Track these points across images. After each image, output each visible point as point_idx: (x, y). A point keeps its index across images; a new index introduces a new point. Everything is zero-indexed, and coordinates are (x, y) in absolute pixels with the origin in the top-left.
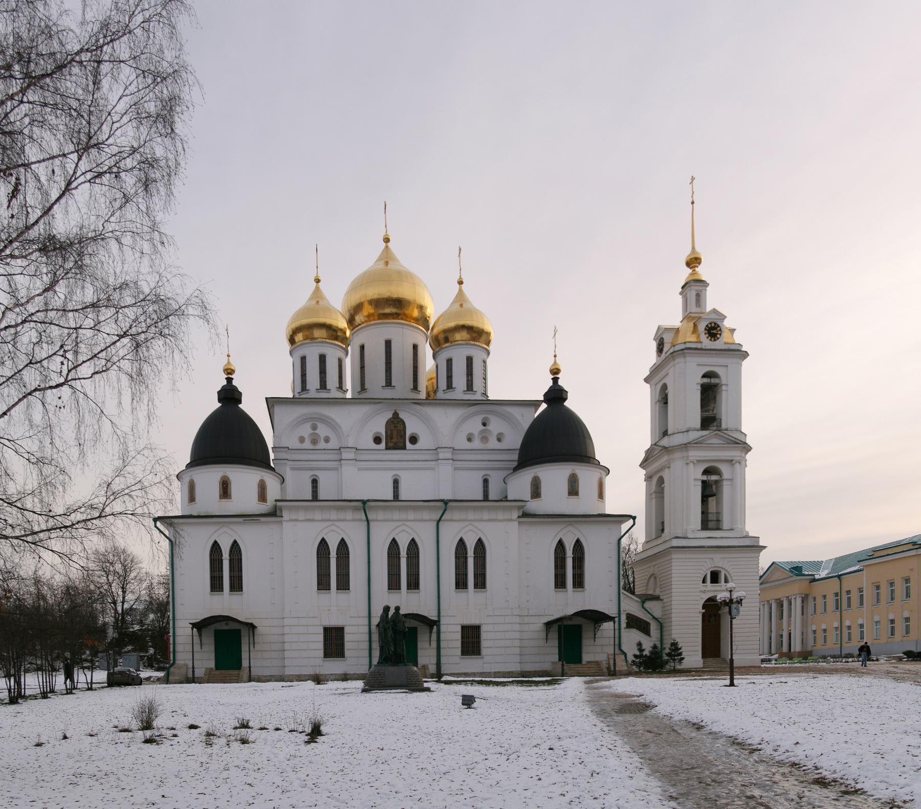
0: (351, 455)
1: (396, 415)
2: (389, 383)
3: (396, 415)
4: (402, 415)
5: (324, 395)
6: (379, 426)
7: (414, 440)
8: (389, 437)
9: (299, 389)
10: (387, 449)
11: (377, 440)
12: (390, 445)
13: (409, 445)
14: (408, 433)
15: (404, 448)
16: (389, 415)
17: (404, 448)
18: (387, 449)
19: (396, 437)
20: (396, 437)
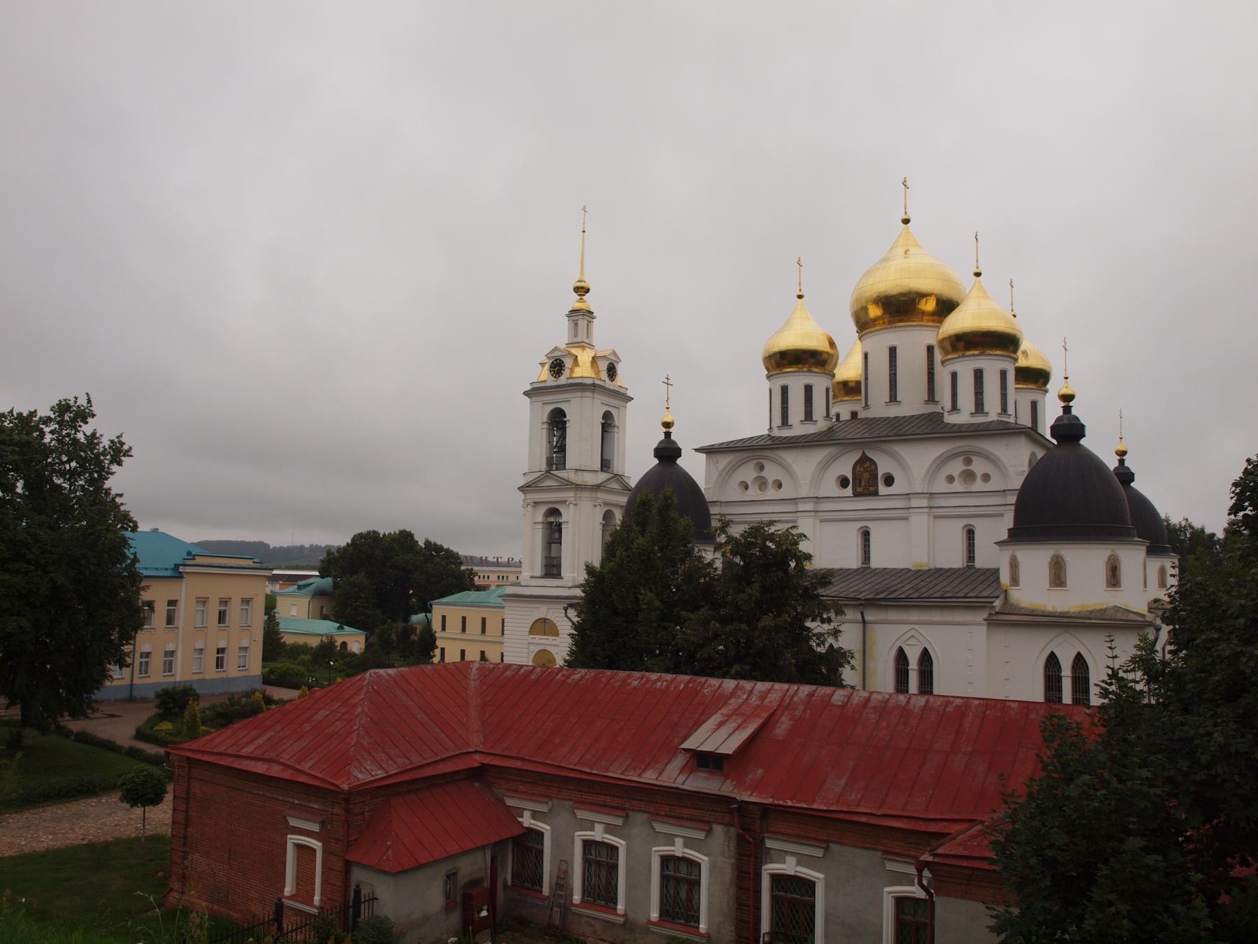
0: (809, 507)
1: (864, 454)
2: (893, 398)
3: (864, 454)
4: (870, 455)
5: (786, 433)
6: (845, 467)
7: (889, 480)
9: (777, 421)
10: (856, 494)
11: (844, 482)
12: (859, 490)
13: (883, 489)
14: (881, 472)
15: (876, 493)
16: (856, 456)
17: (876, 493)
18: (856, 494)
19: (865, 481)
20: (865, 481)
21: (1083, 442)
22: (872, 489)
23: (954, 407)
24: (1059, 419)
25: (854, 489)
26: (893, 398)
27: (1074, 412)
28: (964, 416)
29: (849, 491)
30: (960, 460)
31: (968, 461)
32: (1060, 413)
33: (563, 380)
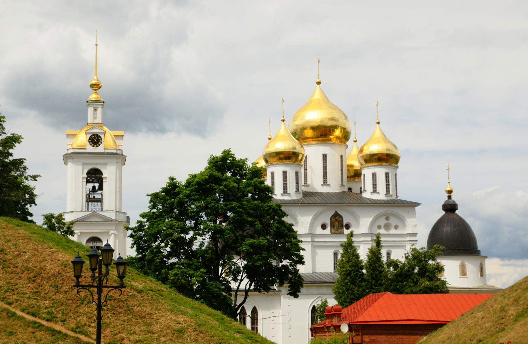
0: (309, 239)
1: (336, 212)
3: (336, 212)
4: (339, 212)
7: (348, 227)
8: (332, 225)
11: (324, 227)
12: (334, 231)
16: (333, 213)
18: (332, 233)
21: (457, 212)
22: (340, 230)
23: (375, 190)
24: (446, 201)
25: (331, 230)
26: (325, 182)
27: (453, 198)
28: (381, 196)
29: (328, 231)
30: (384, 218)
31: (387, 219)
32: (447, 198)
33: (100, 149)
